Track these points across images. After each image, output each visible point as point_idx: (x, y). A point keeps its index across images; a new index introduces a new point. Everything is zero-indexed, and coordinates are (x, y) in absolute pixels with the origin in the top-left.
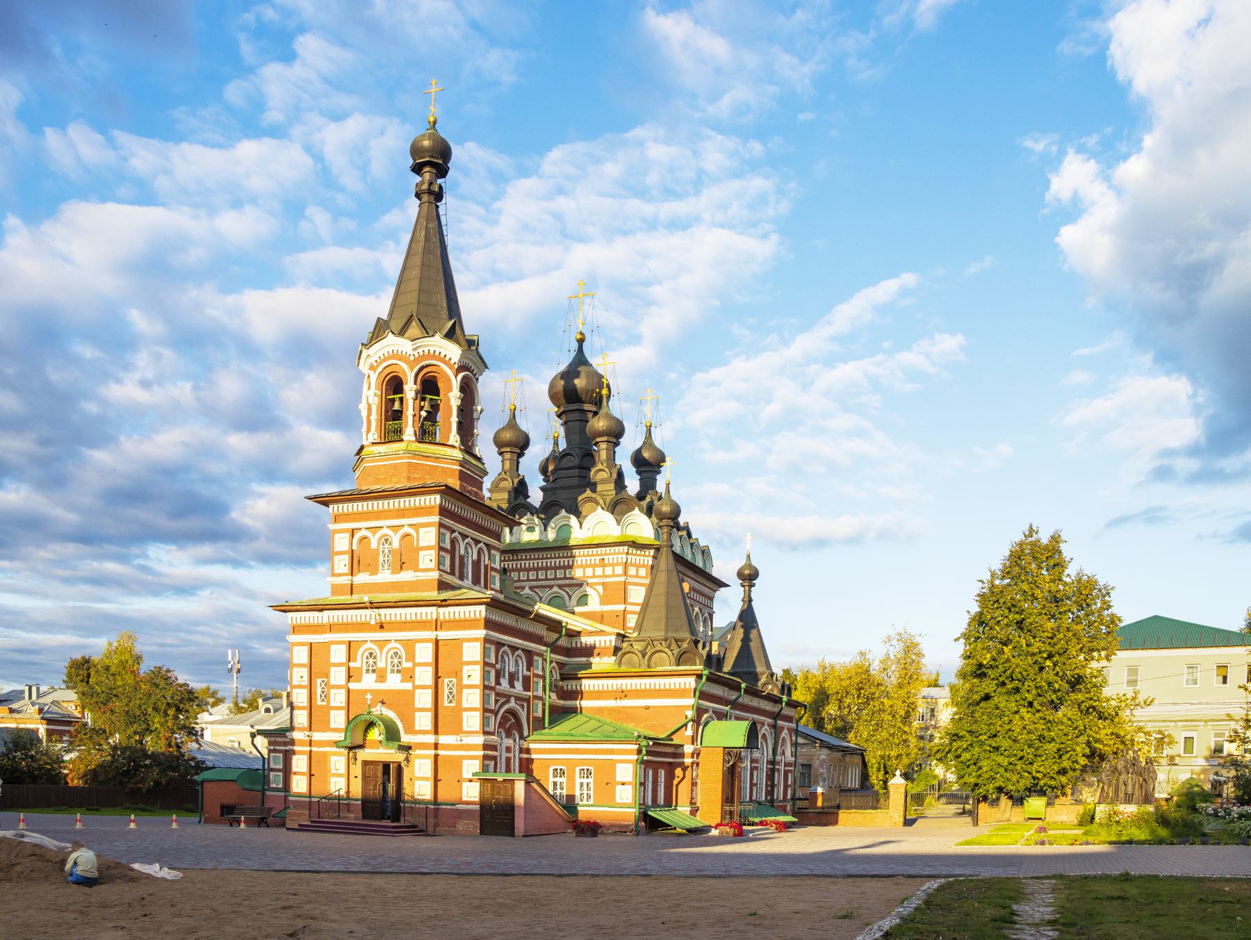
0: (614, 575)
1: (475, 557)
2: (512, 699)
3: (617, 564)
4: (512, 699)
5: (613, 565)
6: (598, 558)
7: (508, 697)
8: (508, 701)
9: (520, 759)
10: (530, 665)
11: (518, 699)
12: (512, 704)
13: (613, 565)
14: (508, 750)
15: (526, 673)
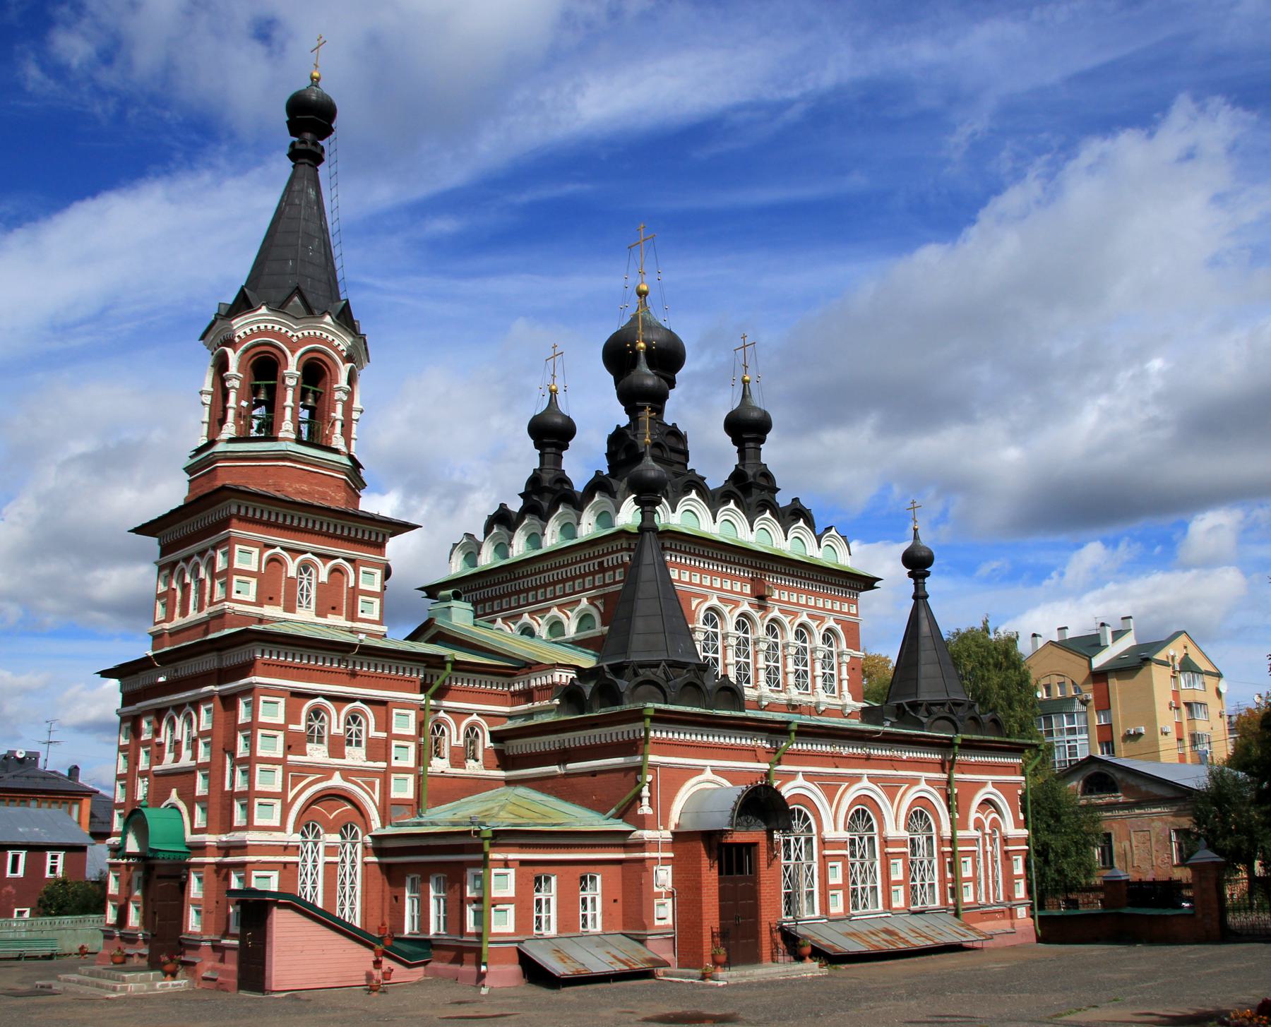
0: (615, 583)
1: (324, 577)
2: (337, 774)
3: (619, 566)
4: (337, 774)
5: (614, 568)
6: (596, 561)
7: (327, 772)
8: (329, 778)
9: (365, 864)
10: (385, 724)
11: (347, 773)
12: (337, 781)
13: (614, 568)
14: (330, 850)
15: (373, 733)
